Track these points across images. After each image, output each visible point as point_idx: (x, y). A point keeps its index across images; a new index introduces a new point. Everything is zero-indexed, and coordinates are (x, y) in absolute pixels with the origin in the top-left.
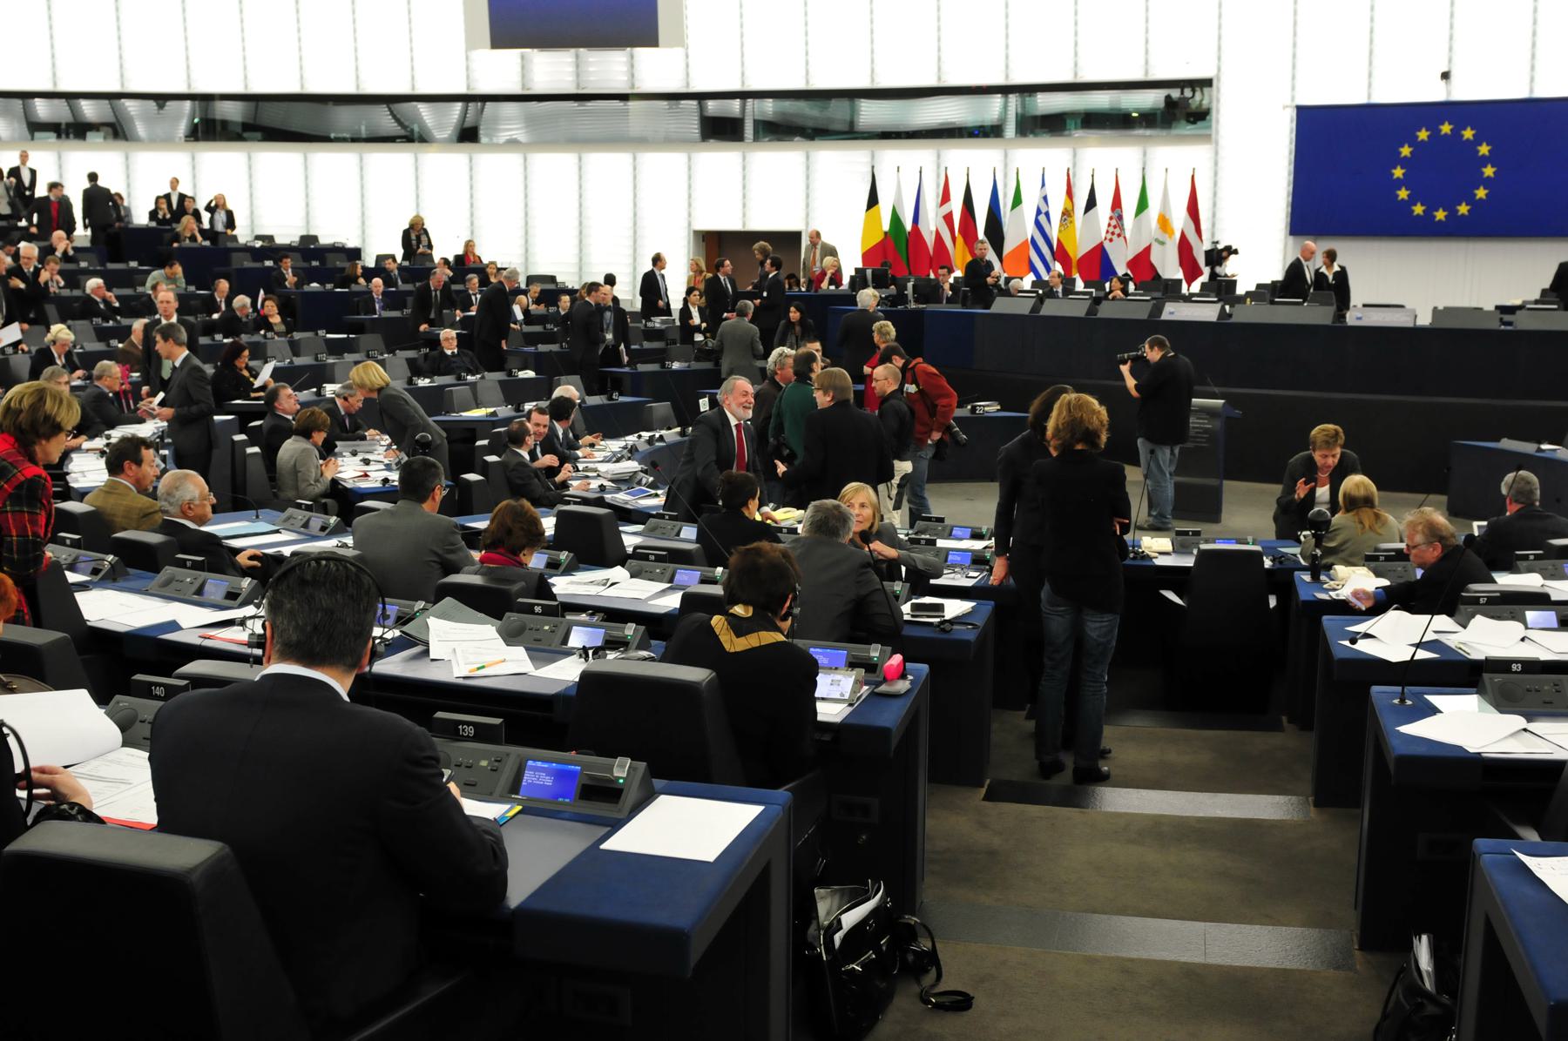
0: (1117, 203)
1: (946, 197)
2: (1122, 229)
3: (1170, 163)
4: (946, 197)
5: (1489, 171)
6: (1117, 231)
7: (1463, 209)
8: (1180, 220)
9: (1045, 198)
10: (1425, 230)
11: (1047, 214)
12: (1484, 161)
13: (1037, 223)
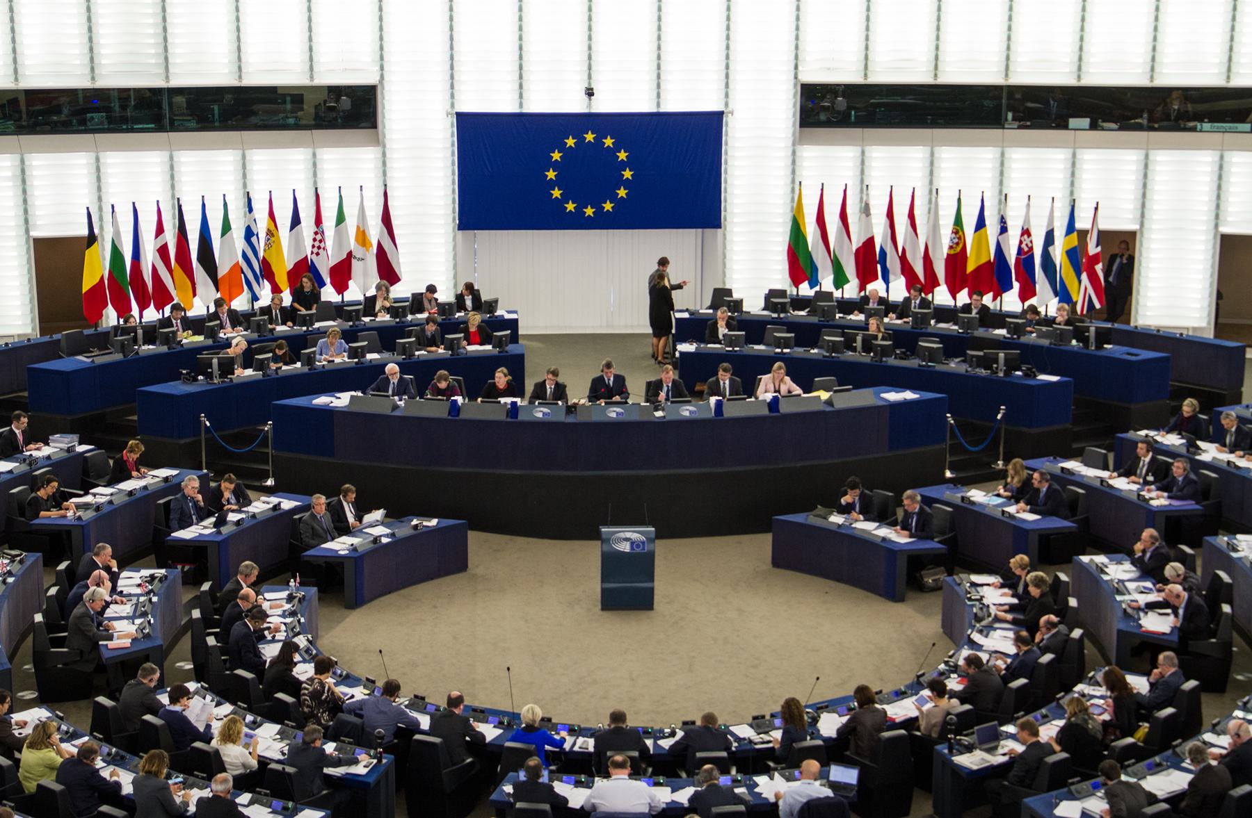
0: (318, 221)
1: (160, 230)
4: (160, 230)
5: (628, 174)
7: (608, 206)
8: (375, 231)
10: (577, 222)
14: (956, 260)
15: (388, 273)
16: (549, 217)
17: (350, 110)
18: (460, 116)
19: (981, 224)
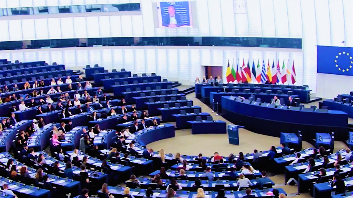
2: (280, 71)
6: (279, 72)
8: (291, 71)
9: (264, 65)
11: (264, 69)
13: (262, 70)
15: (294, 81)
18: (318, 46)
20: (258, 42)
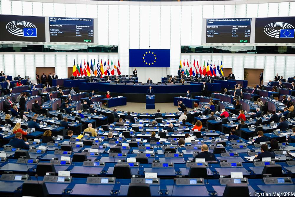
0: (108, 63)
3: (112, 57)
4: (85, 64)
8: (117, 66)
11: (99, 66)
12: (155, 57)
14: (205, 70)
15: (119, 73)
16: (143, 65)
17: (115, 49)
19: (208, 65)
20: (73, 51)
